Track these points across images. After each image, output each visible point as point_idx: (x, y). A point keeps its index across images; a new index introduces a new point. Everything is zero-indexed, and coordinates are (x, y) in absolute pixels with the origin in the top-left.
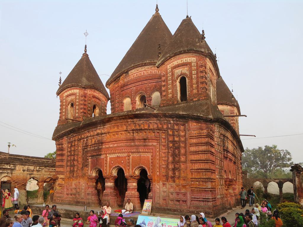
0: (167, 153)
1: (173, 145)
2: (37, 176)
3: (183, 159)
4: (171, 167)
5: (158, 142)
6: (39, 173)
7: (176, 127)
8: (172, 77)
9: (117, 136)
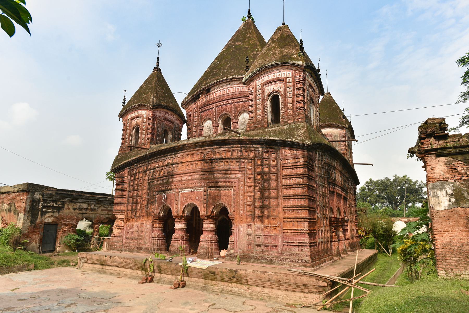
0: (253, 187)
1: (261, 177)
2: (91, 216)
3: (273, 194)
4: (258, 203)
5: (242, 174)
6: (95, 212)
7: (265, 155)
8: (262, 96)
9: (191, 166)
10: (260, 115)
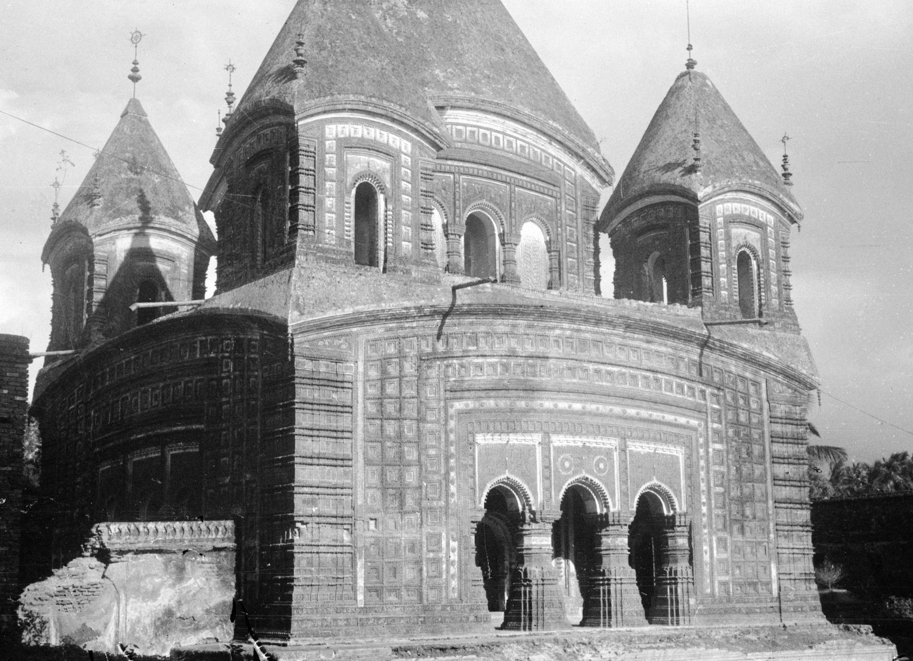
1: (737, 433)
5: (701, 419)
10: (725, 289)
